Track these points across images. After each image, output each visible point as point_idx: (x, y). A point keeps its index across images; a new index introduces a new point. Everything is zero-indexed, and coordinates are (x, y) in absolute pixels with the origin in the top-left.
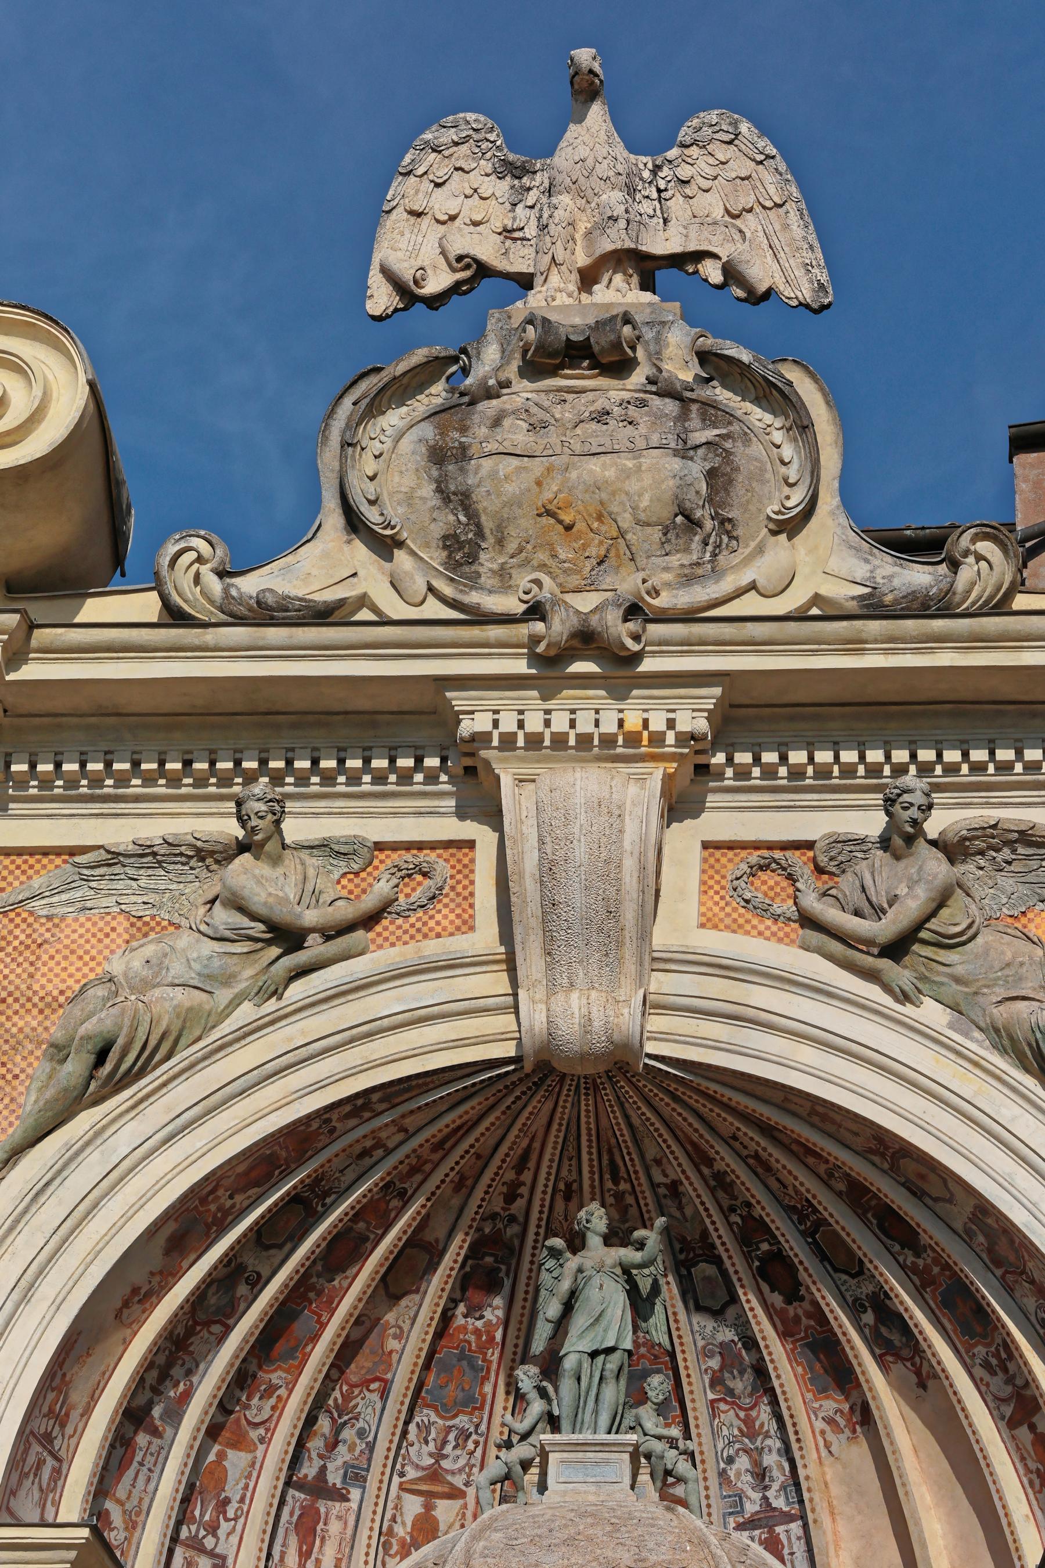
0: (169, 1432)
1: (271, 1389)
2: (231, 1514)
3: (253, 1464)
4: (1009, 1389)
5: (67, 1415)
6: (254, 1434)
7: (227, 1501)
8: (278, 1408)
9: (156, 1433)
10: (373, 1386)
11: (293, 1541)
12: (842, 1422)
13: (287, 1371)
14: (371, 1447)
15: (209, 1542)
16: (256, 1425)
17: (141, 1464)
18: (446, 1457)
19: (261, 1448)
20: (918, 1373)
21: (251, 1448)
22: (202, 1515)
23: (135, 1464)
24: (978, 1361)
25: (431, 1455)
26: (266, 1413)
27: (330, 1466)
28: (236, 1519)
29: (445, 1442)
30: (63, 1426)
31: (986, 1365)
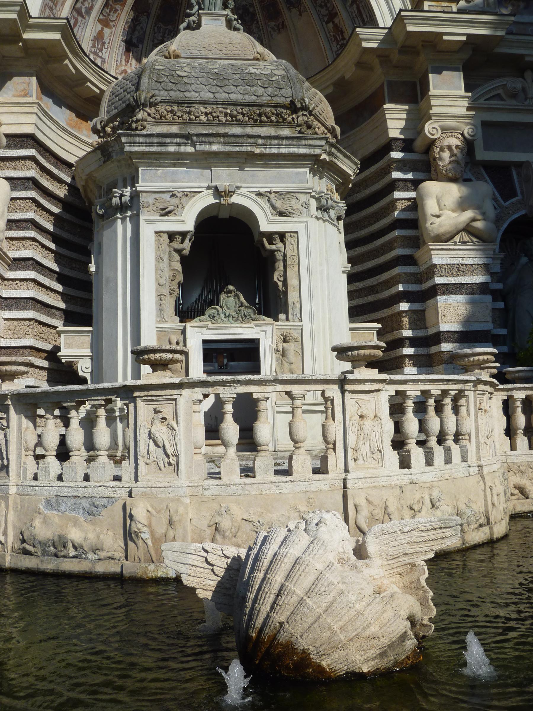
0: (87, 18)
1: (116, 11)
2: (106, 47)
3: (112, 33)
4: (327, 12)
5: (57, 3)
6: (112, 24)
7: (104, 43)
8: (118, 16)
9: (83, 17)
10: (145, 14)
11: (124, 58)
12: (276, 28)
13: (120, 5)
14: (145, 33)
15: (100, 54)
16: (112, 21)
17: (80, 26)
18: (165, 37)
19: (114, 28)
20: (299, 11)
21: (111, 28)
22: (98, 46)
23: (78, 26)
24: (318, 5)
25: (161, 36)
26: (115, 18)
27: (133, 37)
28: (107, 48)
29: (165, 33)
30: (56, 6)
31: (321, 6)
